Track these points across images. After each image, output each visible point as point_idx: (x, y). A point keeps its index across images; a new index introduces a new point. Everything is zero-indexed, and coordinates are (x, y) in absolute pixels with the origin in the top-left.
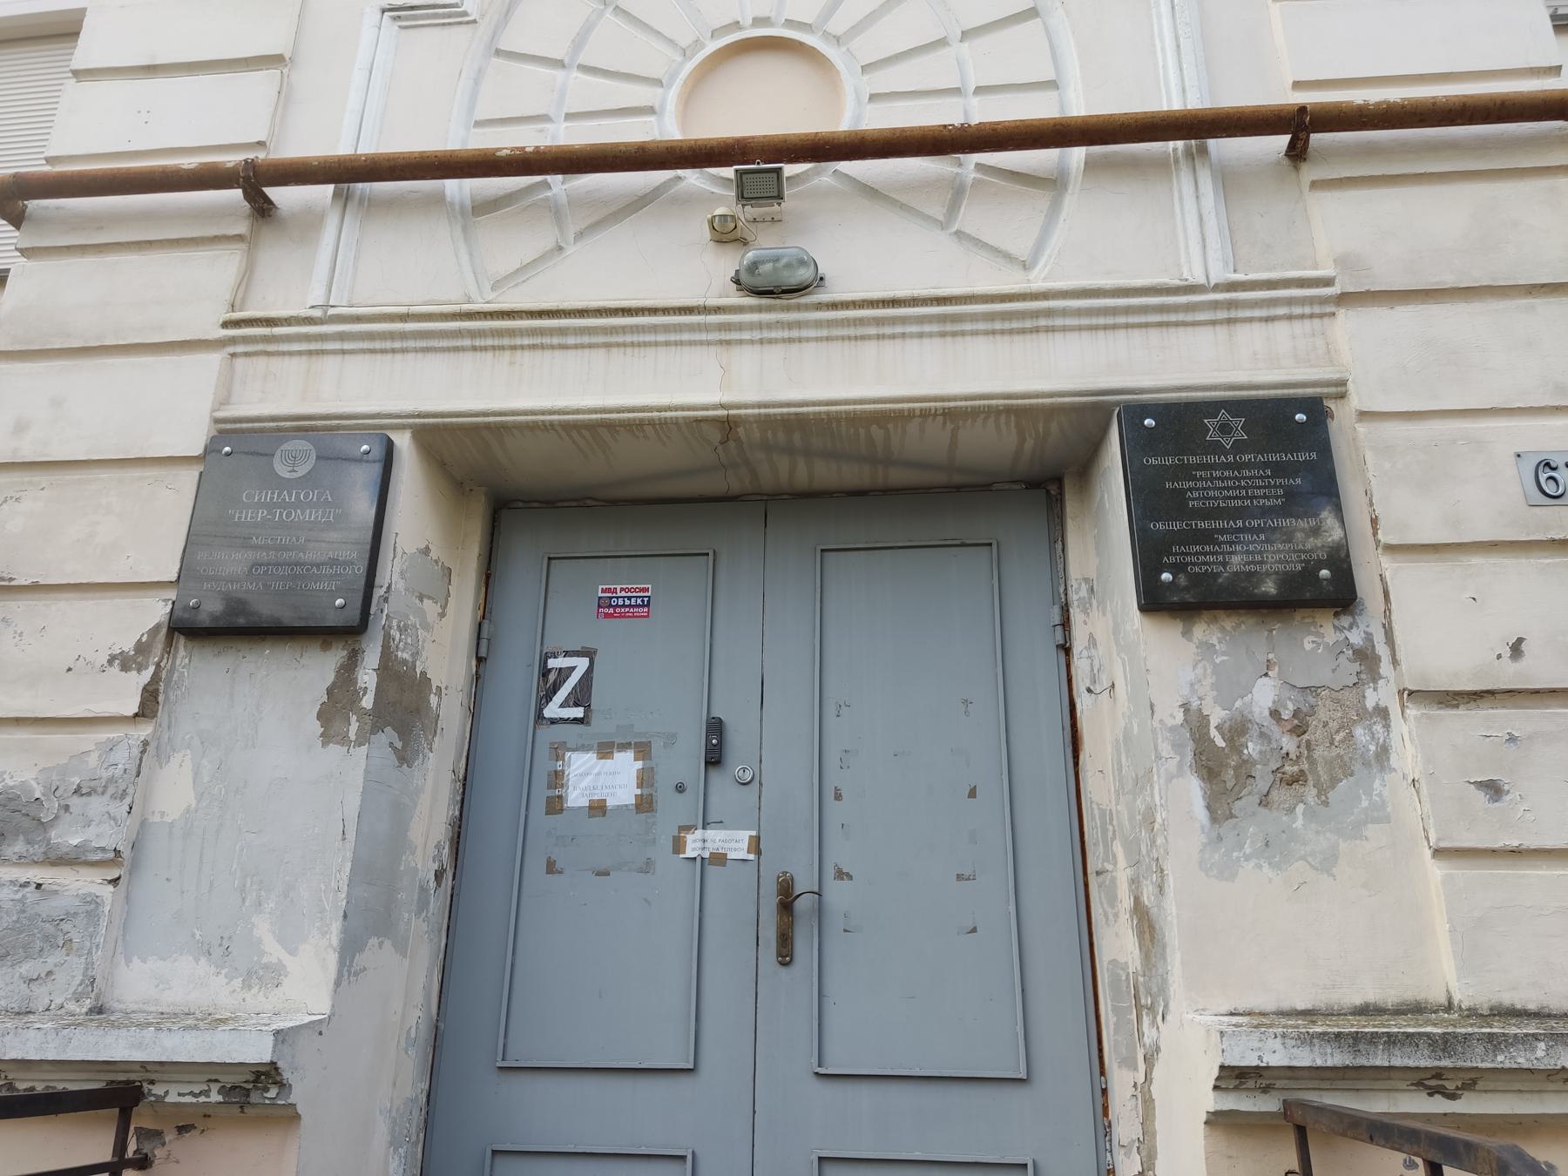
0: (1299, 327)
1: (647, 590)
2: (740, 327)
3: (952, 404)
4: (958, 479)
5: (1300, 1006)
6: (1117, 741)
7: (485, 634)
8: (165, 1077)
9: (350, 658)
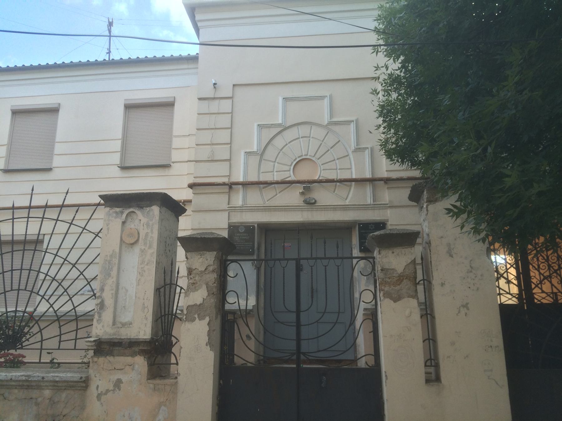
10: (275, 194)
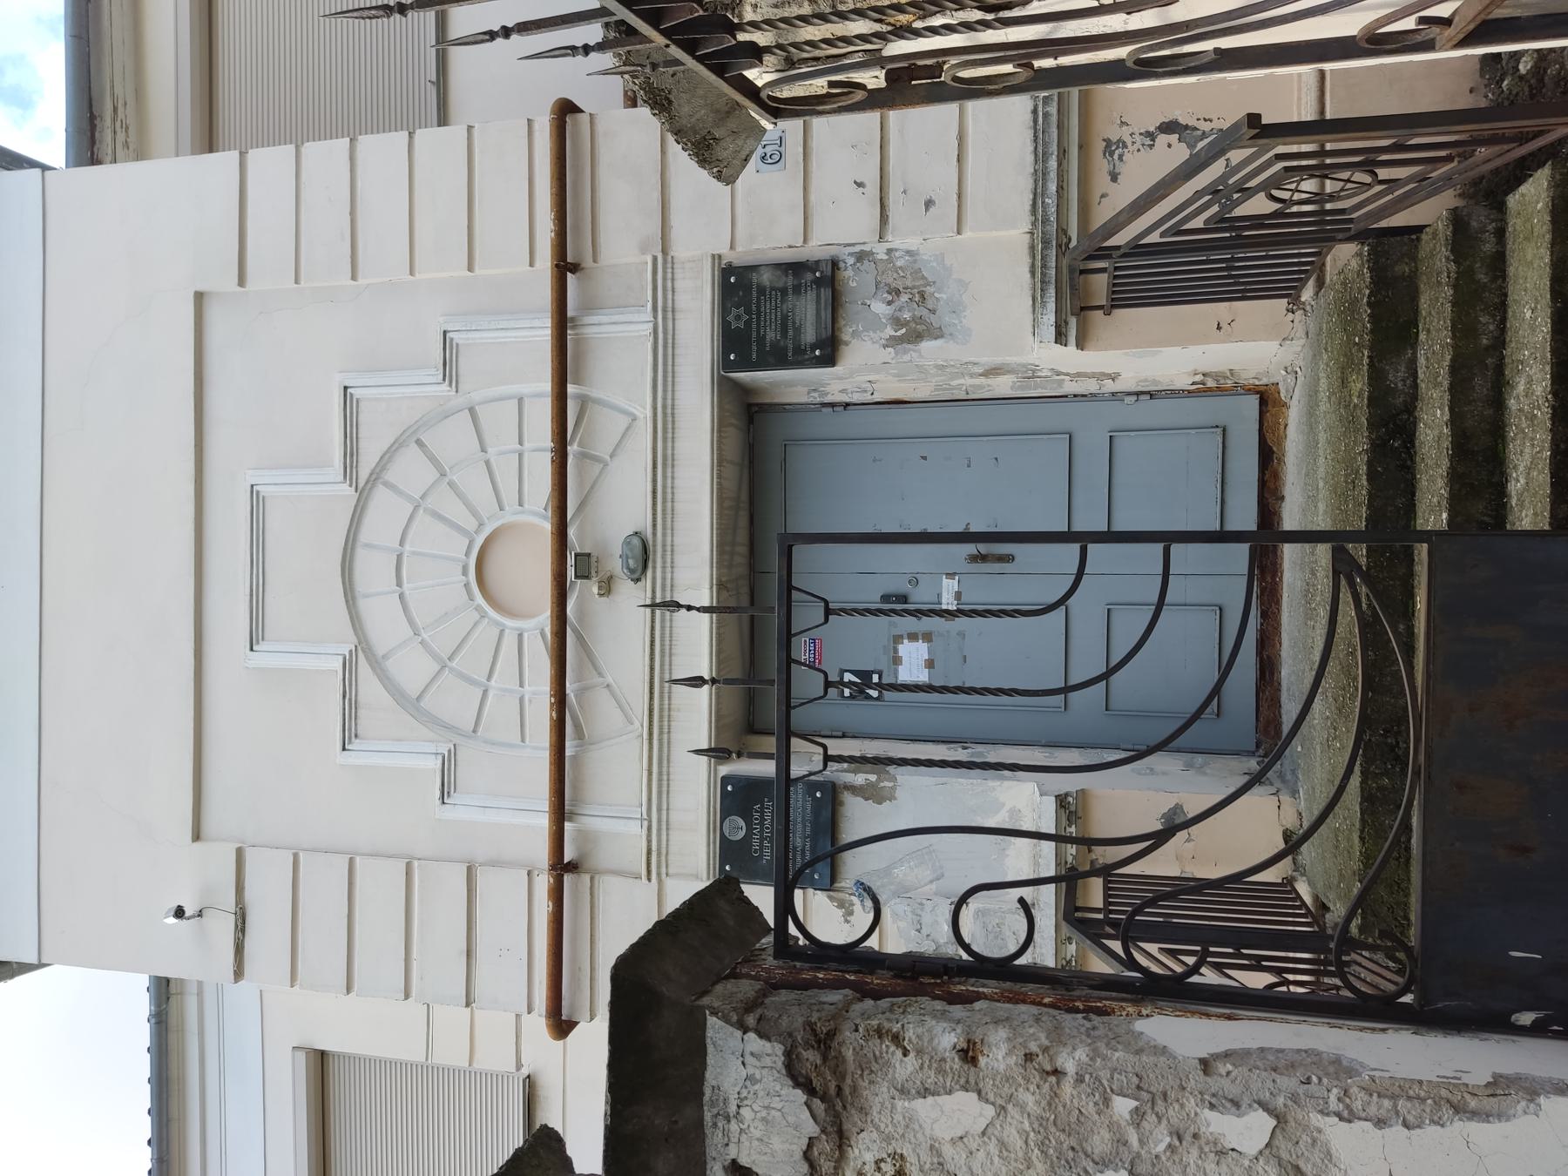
0: (678, 275)
2: (664, 579)
3: (715, 461)
4: (746, 462)
5: (1031, 302)
6: (899, 381)
7: (829, 733)
8: (1063, 855)
9: (848, 790)
10: (606, 690)
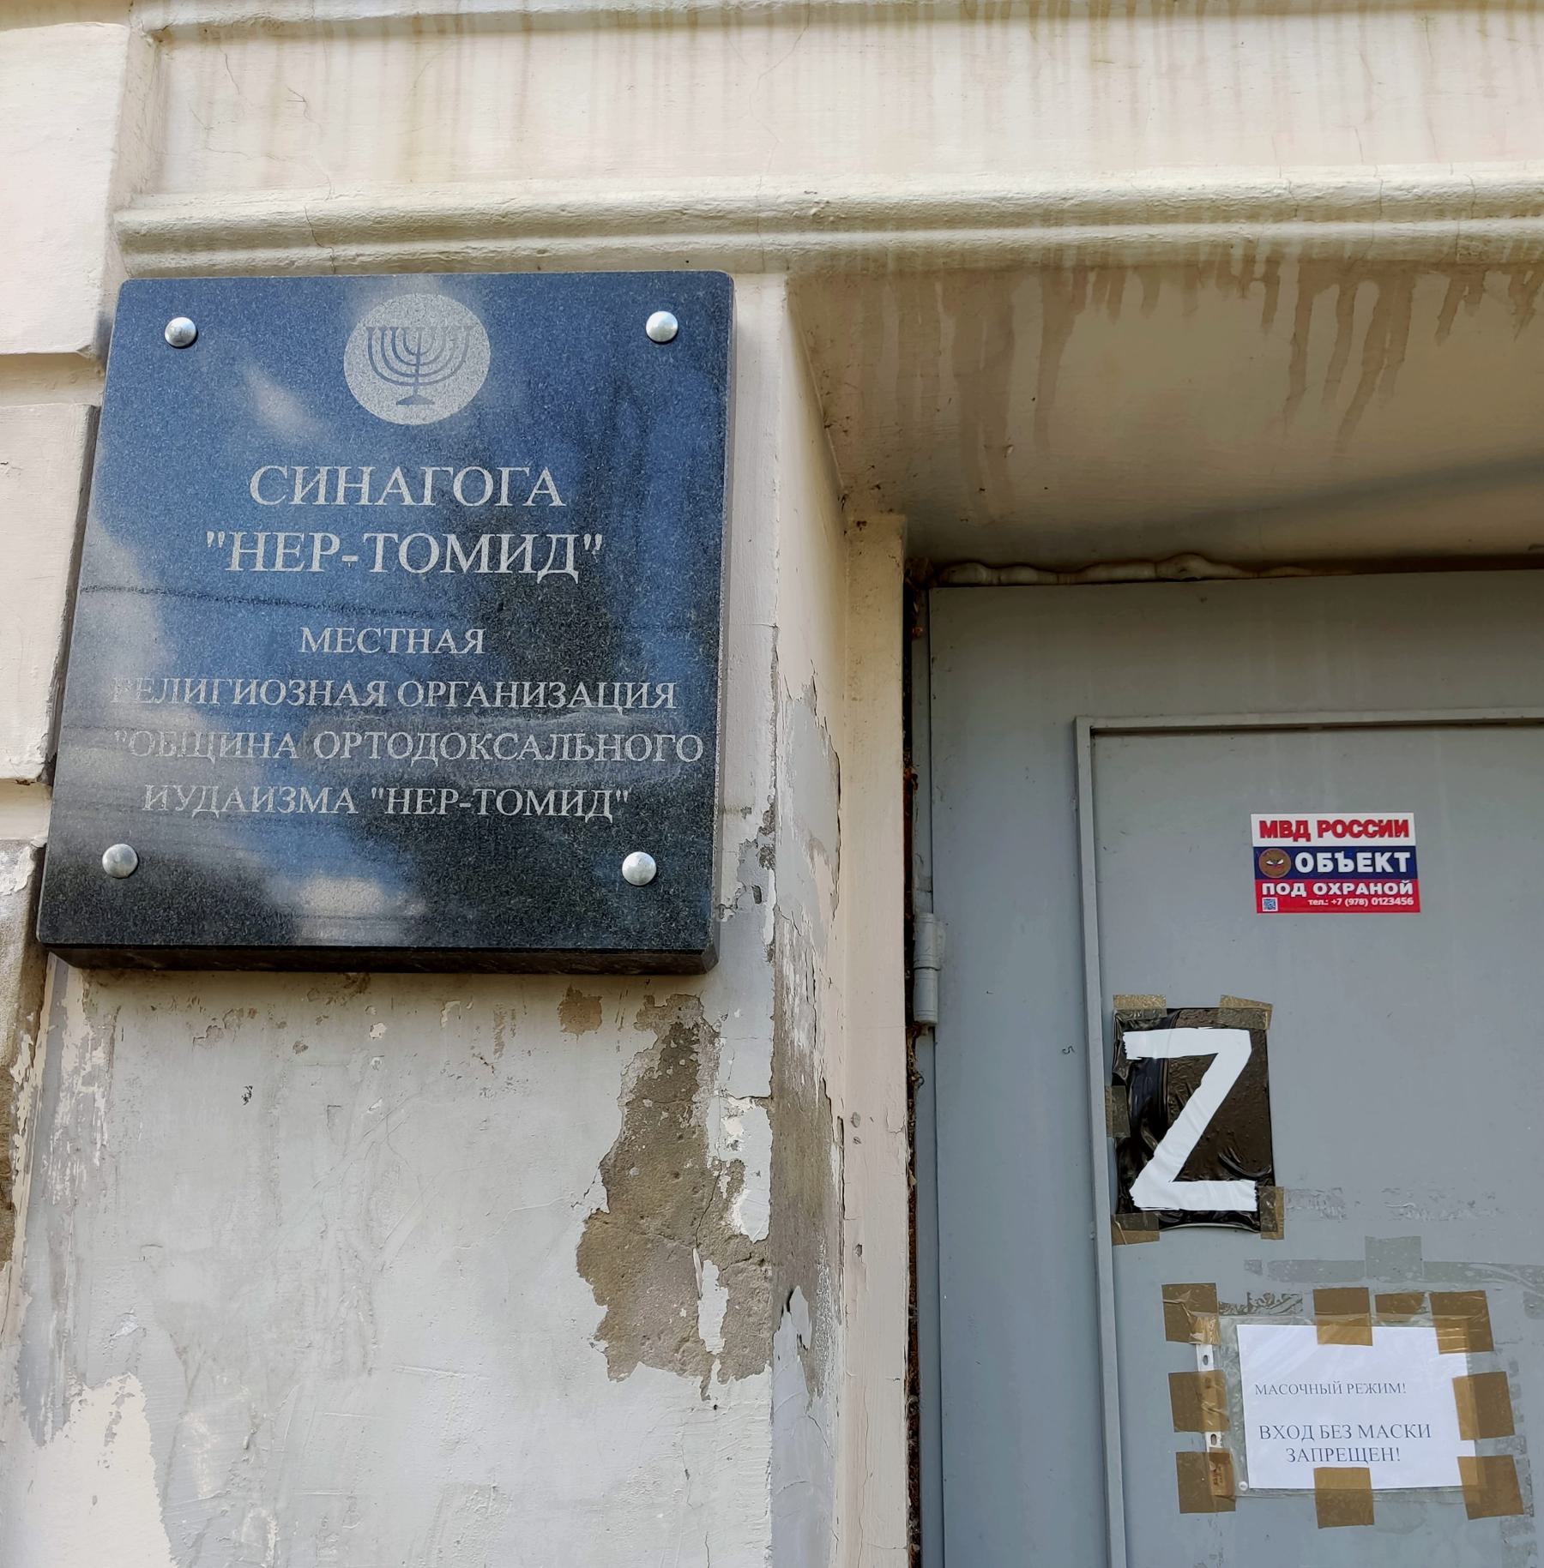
1: (1402, 828)
